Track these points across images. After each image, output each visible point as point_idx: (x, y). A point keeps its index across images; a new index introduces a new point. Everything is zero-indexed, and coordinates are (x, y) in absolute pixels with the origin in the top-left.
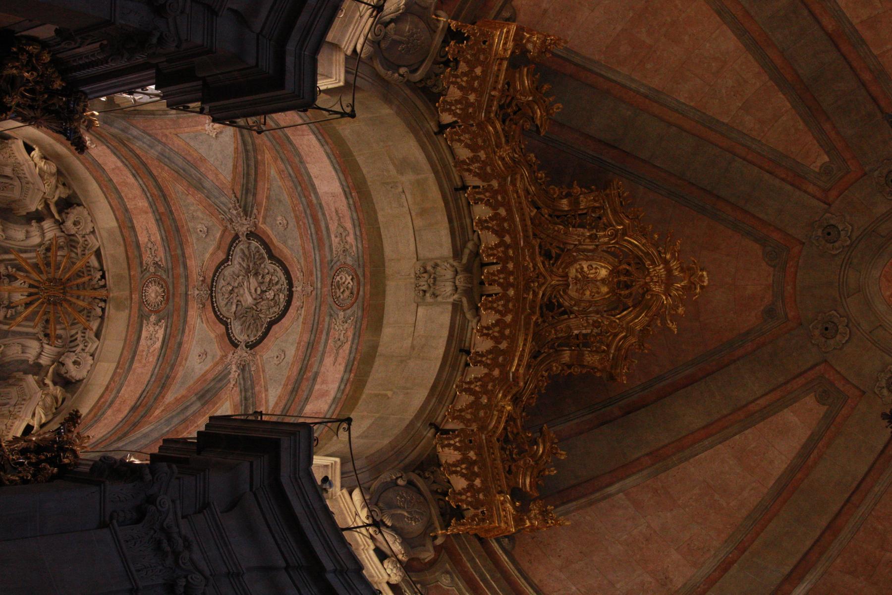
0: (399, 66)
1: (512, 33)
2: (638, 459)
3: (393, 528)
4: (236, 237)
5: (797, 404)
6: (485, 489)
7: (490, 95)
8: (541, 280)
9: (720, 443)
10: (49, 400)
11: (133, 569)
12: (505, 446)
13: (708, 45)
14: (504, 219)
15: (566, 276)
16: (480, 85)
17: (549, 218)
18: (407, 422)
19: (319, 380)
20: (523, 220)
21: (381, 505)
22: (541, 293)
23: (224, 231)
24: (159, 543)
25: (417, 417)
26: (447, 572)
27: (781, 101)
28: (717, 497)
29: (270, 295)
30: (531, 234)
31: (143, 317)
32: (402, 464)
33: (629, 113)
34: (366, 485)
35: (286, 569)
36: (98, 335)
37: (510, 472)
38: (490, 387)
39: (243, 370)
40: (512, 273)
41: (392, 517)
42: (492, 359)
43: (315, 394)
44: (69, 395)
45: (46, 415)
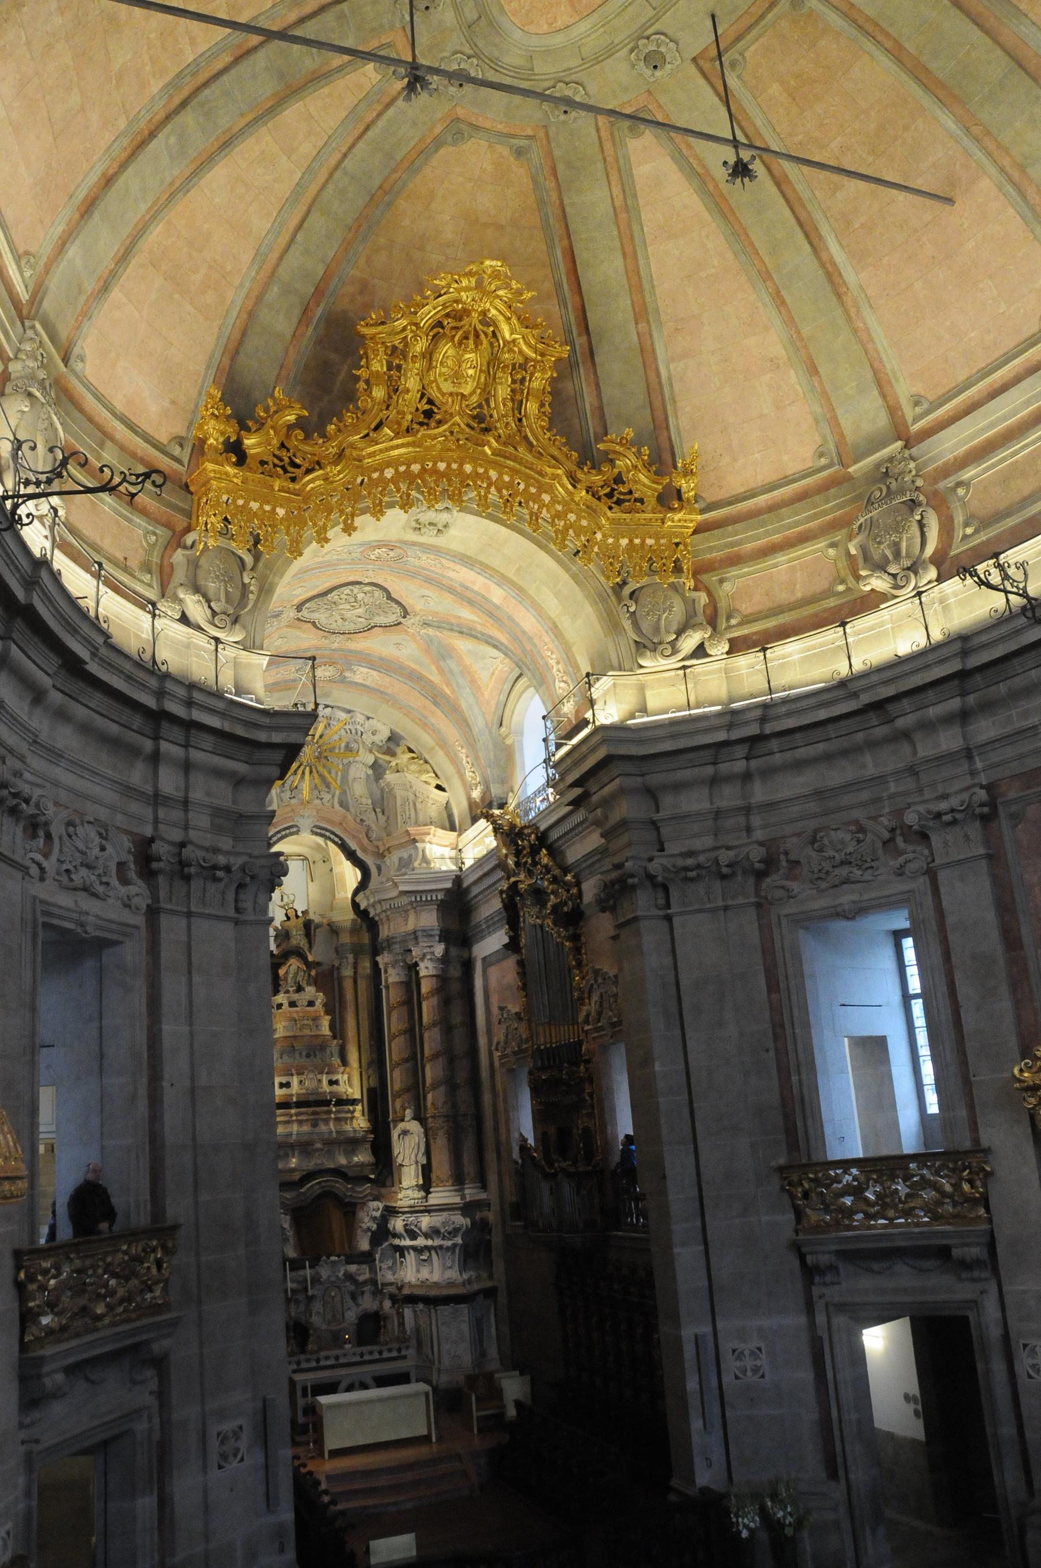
0: (244, 585)
1: (216, 467)
2: (638, 334)
3: (679, 633)
4: (298, 619)
5: (632, 159)
6: (657, 537)
7: (279, 490)
8: (456, 429)
9: (646, 249)
10: (413, 767)
11: (708, 906)
12: (615, 499)
13: (217, 200)
14: (397, 470)
15: (451, 394)
16: (268, 503)
17: (391, 408)
18: (571, 581)
19: (469, 585)
20: (398, 447)
21: (655, 641)
22: (467, 430)
23: (287, 626)
24: (686, 879)
25: (568, 570)
26: (721, 581)
27: (291, 114)
28: (703, 274)
29: (360, 596)
30: (410, 439)
31: (343, 680)
32: (613, 598)
33: (275, 289)
34: (633, 645)
35: (714, 764)
36: (349, 711)
37: (641, 501)
38: (559, 508)
39: (429, 625)
40: (449, 466)
41: (668, 632)
42: (534, 502)
43: (482, 591)
44: (403, 743)
45: (428, 772)
